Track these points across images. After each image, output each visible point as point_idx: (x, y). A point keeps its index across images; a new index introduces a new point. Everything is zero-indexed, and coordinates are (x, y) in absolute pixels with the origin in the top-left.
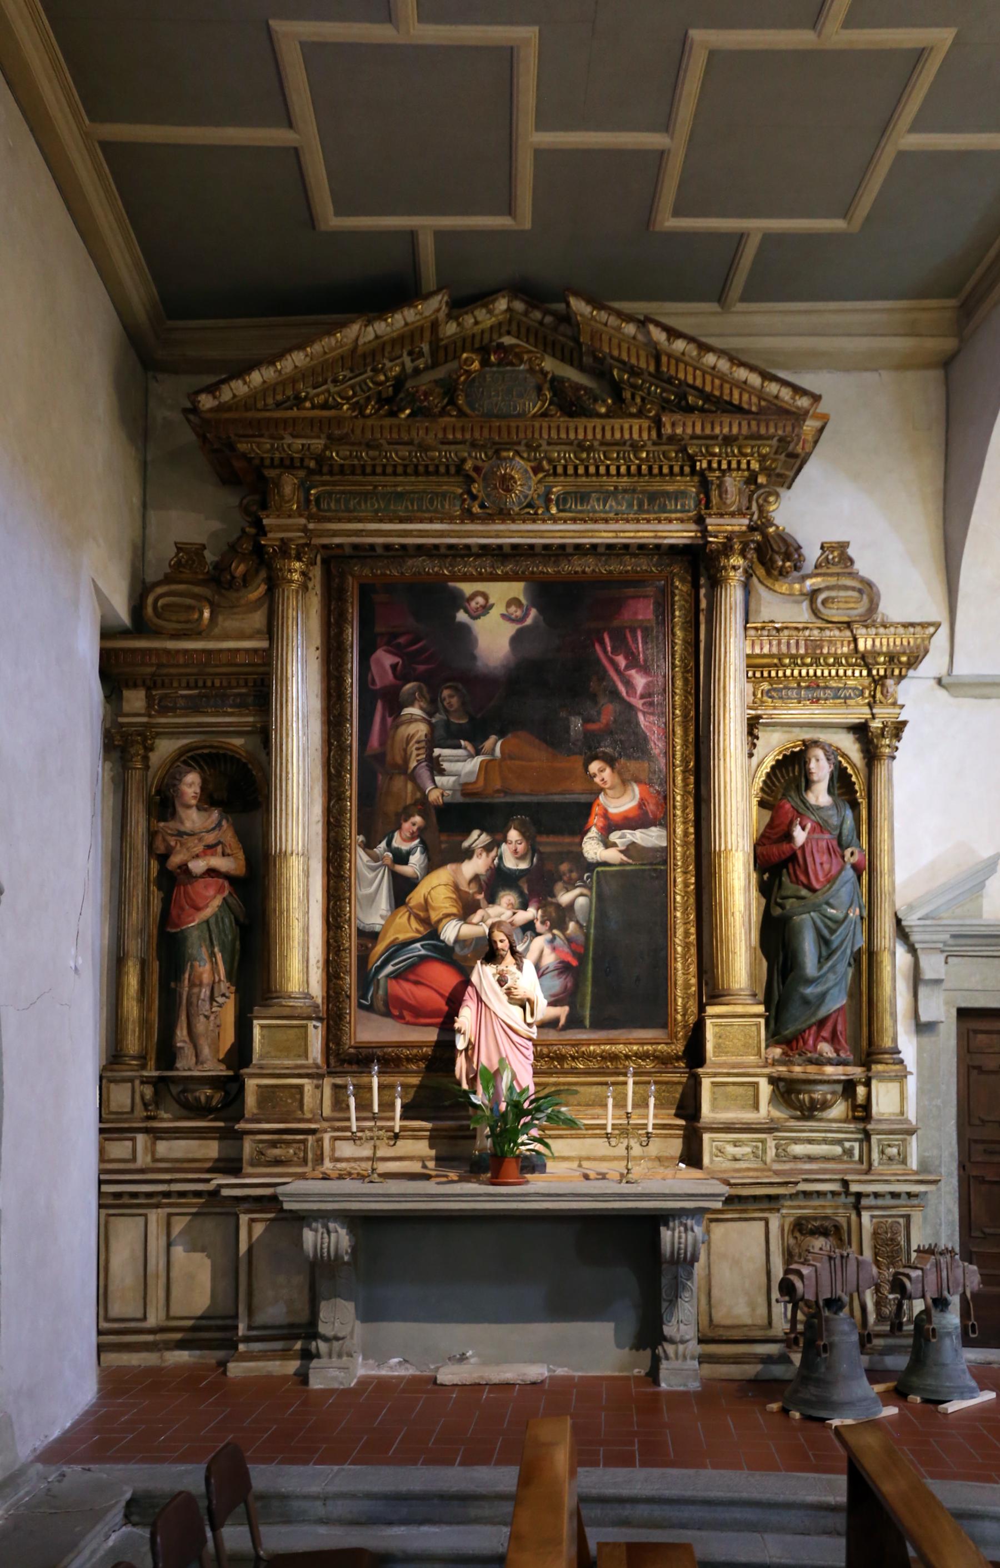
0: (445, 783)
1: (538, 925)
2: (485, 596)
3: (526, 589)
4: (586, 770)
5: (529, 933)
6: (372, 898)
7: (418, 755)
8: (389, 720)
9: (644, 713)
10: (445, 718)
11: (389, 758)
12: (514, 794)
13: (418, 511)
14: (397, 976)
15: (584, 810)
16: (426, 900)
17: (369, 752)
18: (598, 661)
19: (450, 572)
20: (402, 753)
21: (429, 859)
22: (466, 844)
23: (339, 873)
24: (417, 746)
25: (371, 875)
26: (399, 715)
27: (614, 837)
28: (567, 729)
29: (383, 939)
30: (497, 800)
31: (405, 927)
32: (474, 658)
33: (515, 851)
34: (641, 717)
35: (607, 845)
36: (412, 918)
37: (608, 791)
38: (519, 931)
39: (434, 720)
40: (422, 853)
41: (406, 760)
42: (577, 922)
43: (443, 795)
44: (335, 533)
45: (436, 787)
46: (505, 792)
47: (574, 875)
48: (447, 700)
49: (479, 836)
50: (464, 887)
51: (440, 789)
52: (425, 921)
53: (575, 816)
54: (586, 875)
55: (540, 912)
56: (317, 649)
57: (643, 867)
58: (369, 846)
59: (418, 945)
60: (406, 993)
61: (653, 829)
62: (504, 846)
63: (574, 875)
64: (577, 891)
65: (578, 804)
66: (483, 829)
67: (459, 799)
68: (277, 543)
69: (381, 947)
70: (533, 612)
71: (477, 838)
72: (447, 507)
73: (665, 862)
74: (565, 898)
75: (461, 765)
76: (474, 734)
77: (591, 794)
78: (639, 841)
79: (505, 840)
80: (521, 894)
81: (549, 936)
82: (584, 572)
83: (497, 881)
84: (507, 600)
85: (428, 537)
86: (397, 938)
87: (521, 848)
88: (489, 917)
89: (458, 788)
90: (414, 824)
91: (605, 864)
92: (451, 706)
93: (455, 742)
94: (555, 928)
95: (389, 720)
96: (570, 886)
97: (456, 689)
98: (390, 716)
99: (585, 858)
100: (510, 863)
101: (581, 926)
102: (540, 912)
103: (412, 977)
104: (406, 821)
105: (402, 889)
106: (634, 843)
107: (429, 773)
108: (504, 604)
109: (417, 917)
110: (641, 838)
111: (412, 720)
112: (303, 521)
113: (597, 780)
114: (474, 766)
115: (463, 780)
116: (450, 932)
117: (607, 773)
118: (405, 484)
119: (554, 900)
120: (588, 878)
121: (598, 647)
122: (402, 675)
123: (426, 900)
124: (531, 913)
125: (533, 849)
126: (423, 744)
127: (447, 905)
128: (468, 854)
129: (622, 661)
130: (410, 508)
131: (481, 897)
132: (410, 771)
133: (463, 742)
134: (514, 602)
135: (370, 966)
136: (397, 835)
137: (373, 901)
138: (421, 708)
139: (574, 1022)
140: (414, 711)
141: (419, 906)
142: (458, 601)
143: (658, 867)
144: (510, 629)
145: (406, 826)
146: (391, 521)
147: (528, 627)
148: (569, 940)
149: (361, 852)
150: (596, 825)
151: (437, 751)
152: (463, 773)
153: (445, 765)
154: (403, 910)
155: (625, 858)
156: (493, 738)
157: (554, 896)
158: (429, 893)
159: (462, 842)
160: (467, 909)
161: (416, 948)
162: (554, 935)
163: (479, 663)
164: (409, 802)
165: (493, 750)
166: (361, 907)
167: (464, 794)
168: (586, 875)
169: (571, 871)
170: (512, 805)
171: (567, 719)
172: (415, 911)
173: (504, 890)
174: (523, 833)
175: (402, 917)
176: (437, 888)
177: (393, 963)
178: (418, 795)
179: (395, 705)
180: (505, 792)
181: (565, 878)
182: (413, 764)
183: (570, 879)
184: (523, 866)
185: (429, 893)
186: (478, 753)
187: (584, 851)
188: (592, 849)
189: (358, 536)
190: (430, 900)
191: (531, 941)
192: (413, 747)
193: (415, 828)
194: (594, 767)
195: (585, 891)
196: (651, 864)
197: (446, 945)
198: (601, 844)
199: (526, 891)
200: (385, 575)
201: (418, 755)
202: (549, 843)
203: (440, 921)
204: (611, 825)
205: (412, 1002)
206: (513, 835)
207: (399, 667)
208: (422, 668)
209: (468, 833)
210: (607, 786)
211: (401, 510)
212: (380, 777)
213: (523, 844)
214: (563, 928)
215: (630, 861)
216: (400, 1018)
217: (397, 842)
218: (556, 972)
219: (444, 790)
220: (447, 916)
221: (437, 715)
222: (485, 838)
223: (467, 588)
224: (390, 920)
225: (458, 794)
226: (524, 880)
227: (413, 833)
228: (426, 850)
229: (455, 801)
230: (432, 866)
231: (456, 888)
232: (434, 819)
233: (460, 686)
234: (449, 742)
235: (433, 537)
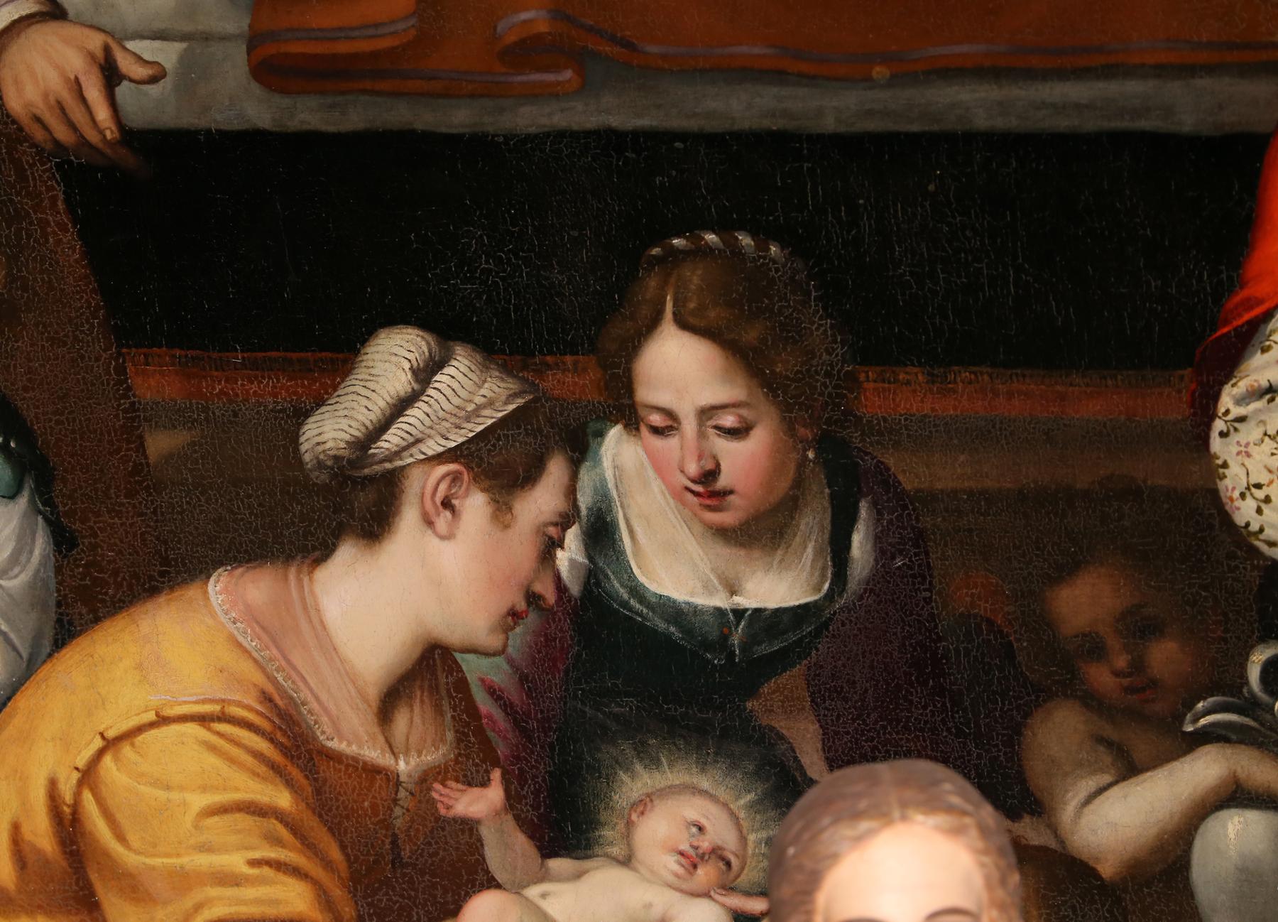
22: (329, 430)
43: (111, 75)
49: (425, 374)
62: (617, 450)
66: (449, 327)
87: (745, 460)
128: (358, 502)
159: (302, 414)
206: (679, 367)
209: (339, 352)
222: (469, 392)
225: (233, 67)
229: (221, 118)
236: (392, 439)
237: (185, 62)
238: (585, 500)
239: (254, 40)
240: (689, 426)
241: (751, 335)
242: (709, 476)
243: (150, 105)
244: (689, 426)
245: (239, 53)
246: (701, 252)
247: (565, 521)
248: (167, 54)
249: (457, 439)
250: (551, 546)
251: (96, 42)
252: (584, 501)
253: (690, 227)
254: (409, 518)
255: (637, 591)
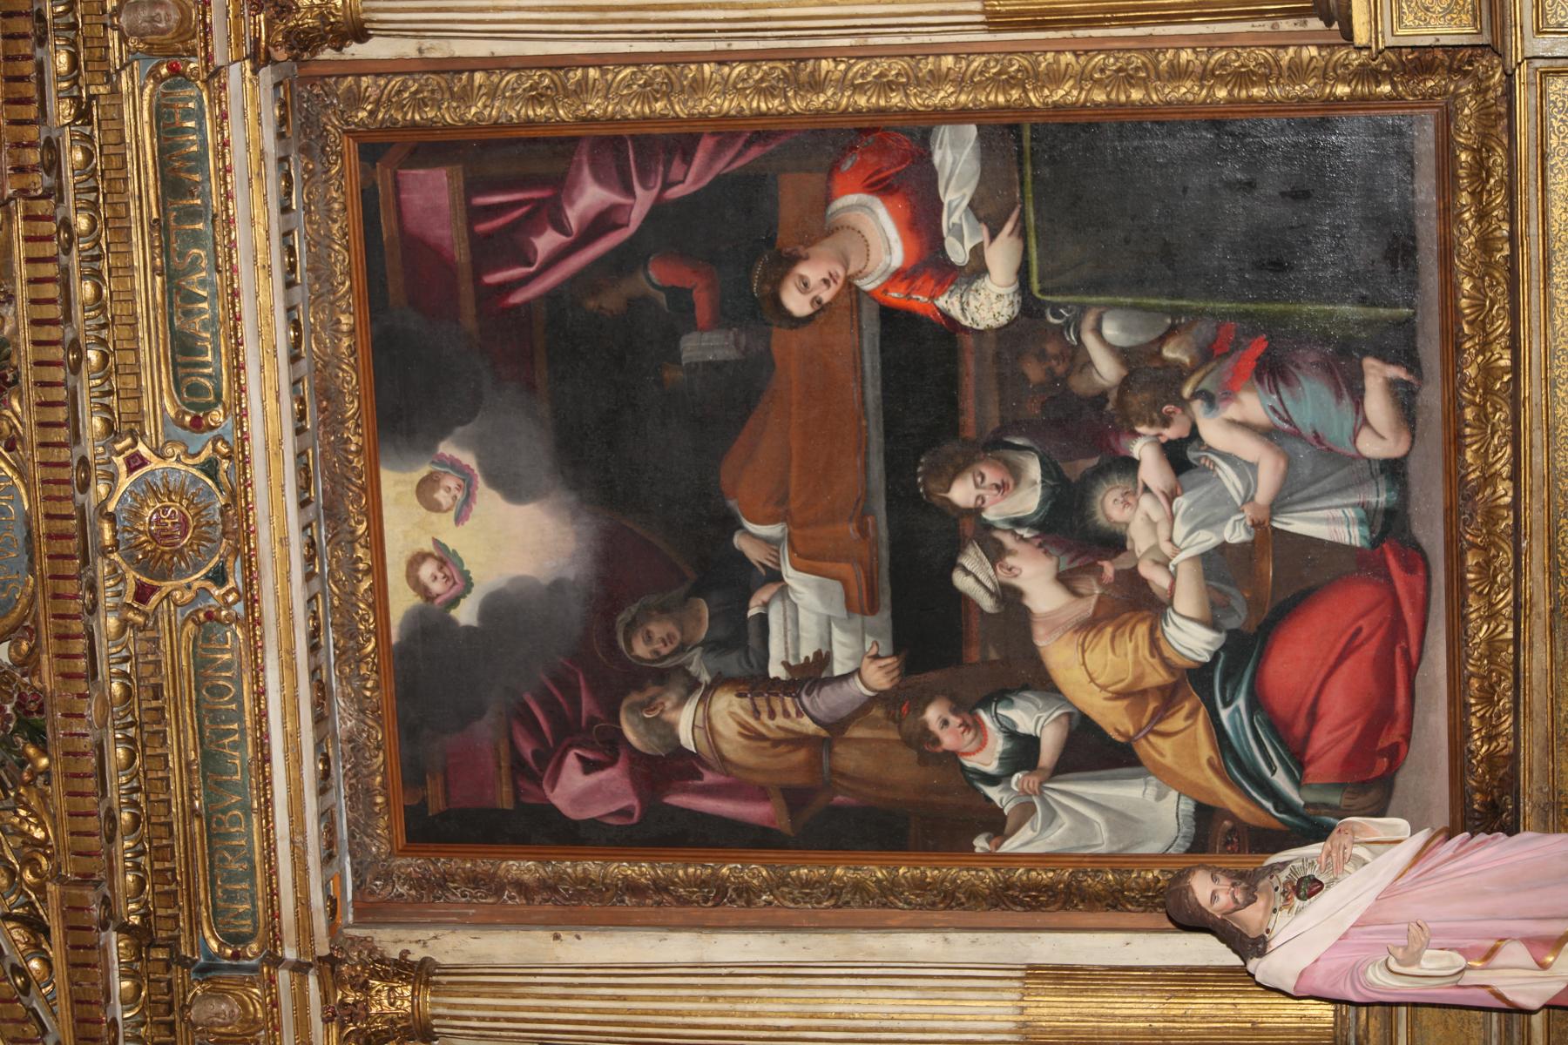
0: (849, 652)
1: (1170, 433)
2: (417, 559)
3: (393, 468)
4: (809, 319)
5: (1192, 455)
6: (1120, 819)
7: (786, 714)
8: (709, 778)
9: (667, 185)
10: (698, 652)
11: (798, 780)
12: (867, 495)
13: (241, 720)
14: (1297, 762)
15: (894, 320)
16: (1119, 695)
17: (783, 824)
18: (551, 296)
19: (369, 640)
20: (782, 749)
21: (1026, 688)
22: (988, 604)
23: (1061, 892)
24: (764, 717)
25: (1065, 820)
26: (696, 756)
27: (958, 253)
28: (717, 366)
29: (1211, 793)
30: (884, 533)
31: (1183, 743)
32: (557, 586)
33: (1001, 487)
34: (675, 192)
35: (978, 268)
36: (1162, 727)
37: (851, 271)
38: (1184, 477)
39: (706, 678)
40: (1011, 704)
41: (798, 740)
42: (1162, 340)
43: (876, 657)
44: (303, 903)
45: (858, 671)
46: (862, 517)
47: (1052, 348)
48: (659, 646)
49: (968, 573)
50: (1087, 607)
51: (861, 660)
52: (1168, 698)
53: (917, 351)
54: (1052, 320)
55: (1142, 429)
56: (557, 937)
57: (1028, 179)
58: (997, 824)
59: (1224, 714)
60: (1338, 741)
61: (937, 159)
62: (990, 515)
63: (1052, 348)
64: (1090, 340)
65: (886, 339)
66: (952, 564)
67: (883, 619)
68: (334, 1031)
69: (1230, 799)
70: (446, 448)
71: (973, 577)
72: (227, 656)
73: (1015, 128)
74: (1107, 370)
75: (807, 615)
76: (732, 583)
77: (859, 310)
78: (969, 192)
79: (976, 512)
80: (1100, 473)
81: (1198, 407)
82: (352, 332)
83: (1073, 532)
84: (423, 511)
85: (296, 697)
86: (1210, 762)
87: (992, 476)
88: (1155, 548)
89: (858, 619)
90: (945, 723)
91: (1023, 273)
92: (670, 637)
93: (753, 629)
94: (1179, 393)
95: (709, 778)
96: (1078, 359)
97: (631, 627)
98: (700, 776)
99: (1011, 322)
100: (1029, 500)
101: (1171, 331)
102: (1142, 429)
103: (1300, 726)
104: (937, 741)
105: (1093, 751)
106: (970, 205)
107: (827, 690)
108: (434, 516)
109: (1162, 714)
110: (959, 188)
111: (707, 727)
112: (283, 976)
113: (826, 295)
114: (806, 585)
115: (839, 611)
116: (1192, 640)
117: (812, 271)
118: (180, 745)
119: (1113, 396)
120: (1056, 315)
121: (518, 298)
122: (606, 748)
123: (1119, 695)
124: (1143, 450)
125: (995, 446)
126: (761, 703)
127: (1130, 646)
128: (1010, 597)
129: (546, 242)
130: (236, 737)
131: (1109, 569)
132: (823, 733)
133: (752, 612)
134: (425, 490)
135: (1277, 825)
136: (969, 762)
137: (1122, 815)
138: (680, 705)
139: (1400, 346)
140: (684, 722)
141: (1135, 711)
142: (430, 624)
143: (1027, 144)
144: (488, 500)
145: (948, 740)
146: (267, 782)
147: (480, 465)
148: (1208, 354)
149: (1010, 846)
150: (933, 297)
151: (776, 670)
152: (822, 610)
153: (807, 651)
154: (1143, 748)
155: (1009, 227)
156: (739, 541)
157: (1103, 396)
158: (1103, 688)
159: (982, 611)
160: (1138, 602)
161: (1231, 718)
162: (1195, 395)
163: (570, 574)
164: (894, 735)
165: (767, 541)
166: (1139, 844)
167: (873, 609)
168: (1052, 320)
169: (1042, 356)
170: (891, 496)
171: (692, 368)
172: (1145, 721)
173: (1094, 513)
174: (957, 472)
175: (1162, 750)
176: (1091, 670)
177: (1268, 773)
178: (877, 712)
179: (669, 767)
180: (862, 517)
181: (1060, 369)
182: (807, 725)
183: (1060, 357)
184: (1034, 470)
185: (1103, 688)
186: (775, 576)
187: (994, 324)
188: (988, 304)
189: (305, 852)
190: (1119, 686)
191: (1210, 449)
192: (770, 725)
193: (955, 721)
194: (796, 302)
195: (1089, 321)
196: (1021, 164)
197: (1223, 648)
198: (978, 284)
199: (1094, 461)
200: (384, 785)
201: (786, 714)
202: (978, 408)
203: (1165, 662)
204: (930, 262)
205: (1358, 726)
206: (962, 493)
207: (589, 755)
208: (587, 705)
209: (960, 598)
210: (841, 272)
211: (239, 759)
212: (839, 798)
213: (984, 470)
214: (1179, 374)
215: (1014, 216)
216: (1395, 756)
217: (987, 760)
218: (1281, 386)
219: (864, 653)
220: (1154, 645)
221: (692, 669)
222: (972, 559)
223: (402, 601)
224: (1168, 778)
226: (1066, 468)
227: (966, 726)
228: (1002, 694)
230: (1041, 683)
231: (1090, 625)
232: (932, 676)
233: (623, 617)
234: (753, 642)
235: (296, 688)
236: (989, 585)
237: (871, 634)
238: (1007, 527)
239: (863, 613)
240: (981, 492)
241: (951, 470)
242: (997, 487)
243: (885, 647)
244: (981, 492)
245: (869, 619)
246: (924, 482)
247: (1014, 534)
248: (869, 641)
249: (988, 564)
250: (1021, 537)
251: (866, 661)
252: (1007, 527)
253: (917, 486)
254: (1016, 582)
255: (1036, 513)
